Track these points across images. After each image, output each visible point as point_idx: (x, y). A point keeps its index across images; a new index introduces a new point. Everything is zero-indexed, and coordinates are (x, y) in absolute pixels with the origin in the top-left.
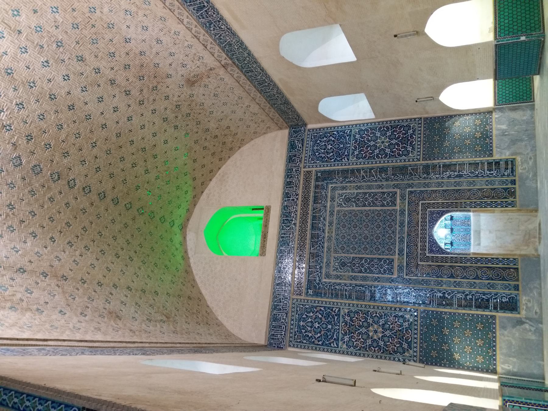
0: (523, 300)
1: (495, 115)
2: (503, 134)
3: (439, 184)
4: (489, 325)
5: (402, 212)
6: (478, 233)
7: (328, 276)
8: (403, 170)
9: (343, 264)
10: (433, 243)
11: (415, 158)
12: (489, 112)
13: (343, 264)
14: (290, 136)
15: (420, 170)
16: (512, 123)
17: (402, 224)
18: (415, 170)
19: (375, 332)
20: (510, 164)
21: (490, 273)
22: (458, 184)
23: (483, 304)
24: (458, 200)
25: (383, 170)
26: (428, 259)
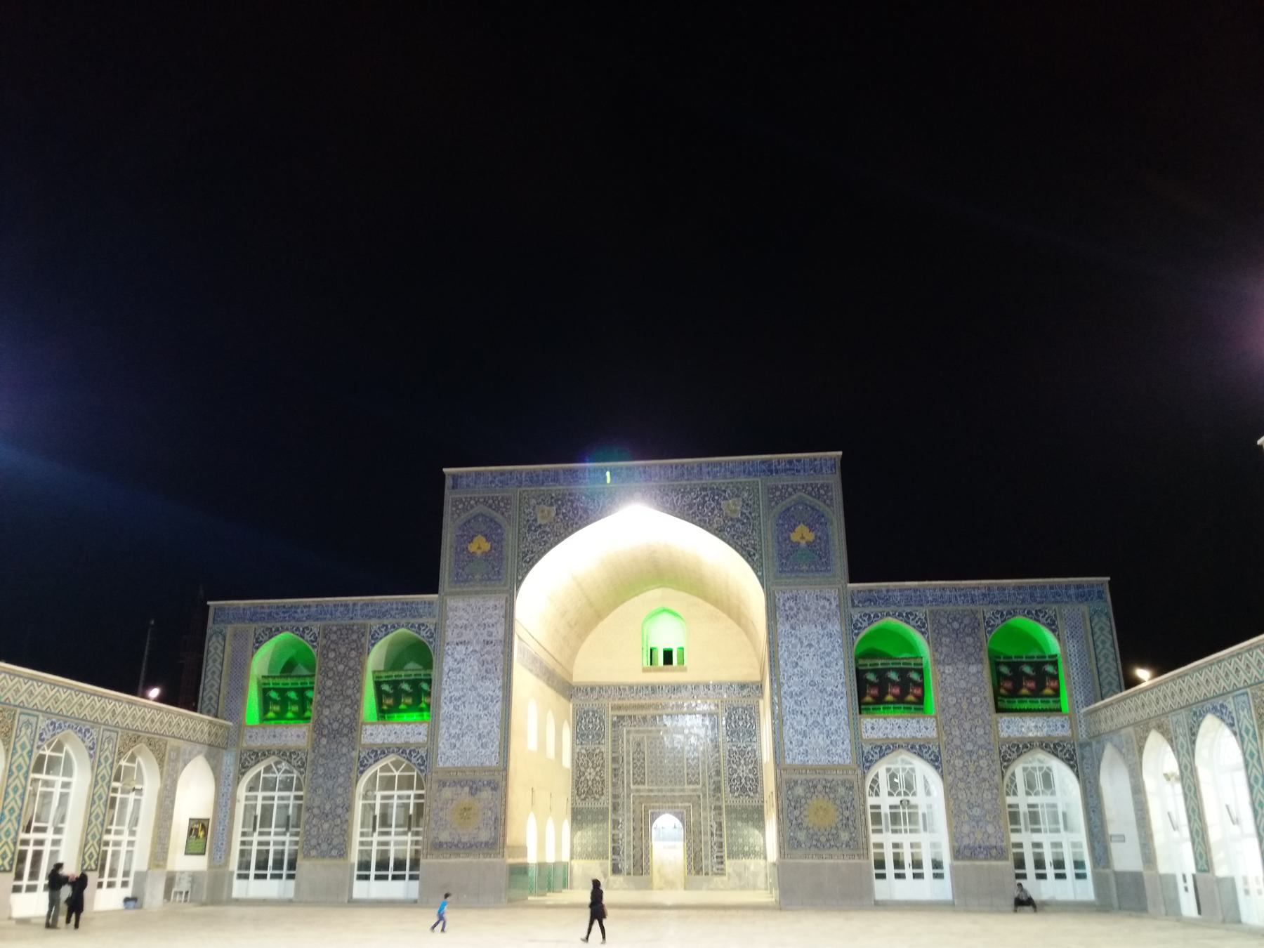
0: (620, 879)
1: (762, 862)
2: (746, 868)
3: (705, 818)
4: (602, 855)
5: (683, 790)
6: (674, 847)
7: (628, 732)
8: (718, 789)
9: (639, 745)
10: (659, 814)
11: (728, 798)
12: (765, 858)
13: (639, 745)
14: (753, 683)
15: (718, 803)
16: (755, 874)
17: (673, 790)
18: (718, 799)
19: (590, 774)
20: (721, 872)
21: (638, 856)
22: (706, 834)
23: (615, 851)
24: (693, 835)
25: (718, 773)
26: (646, 811)
